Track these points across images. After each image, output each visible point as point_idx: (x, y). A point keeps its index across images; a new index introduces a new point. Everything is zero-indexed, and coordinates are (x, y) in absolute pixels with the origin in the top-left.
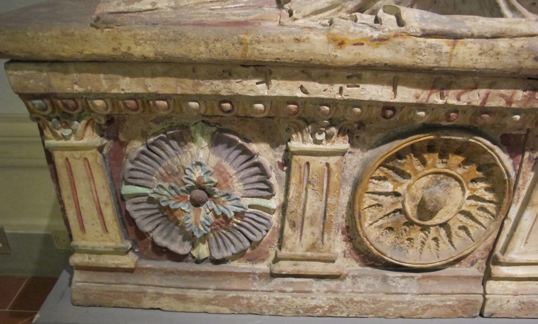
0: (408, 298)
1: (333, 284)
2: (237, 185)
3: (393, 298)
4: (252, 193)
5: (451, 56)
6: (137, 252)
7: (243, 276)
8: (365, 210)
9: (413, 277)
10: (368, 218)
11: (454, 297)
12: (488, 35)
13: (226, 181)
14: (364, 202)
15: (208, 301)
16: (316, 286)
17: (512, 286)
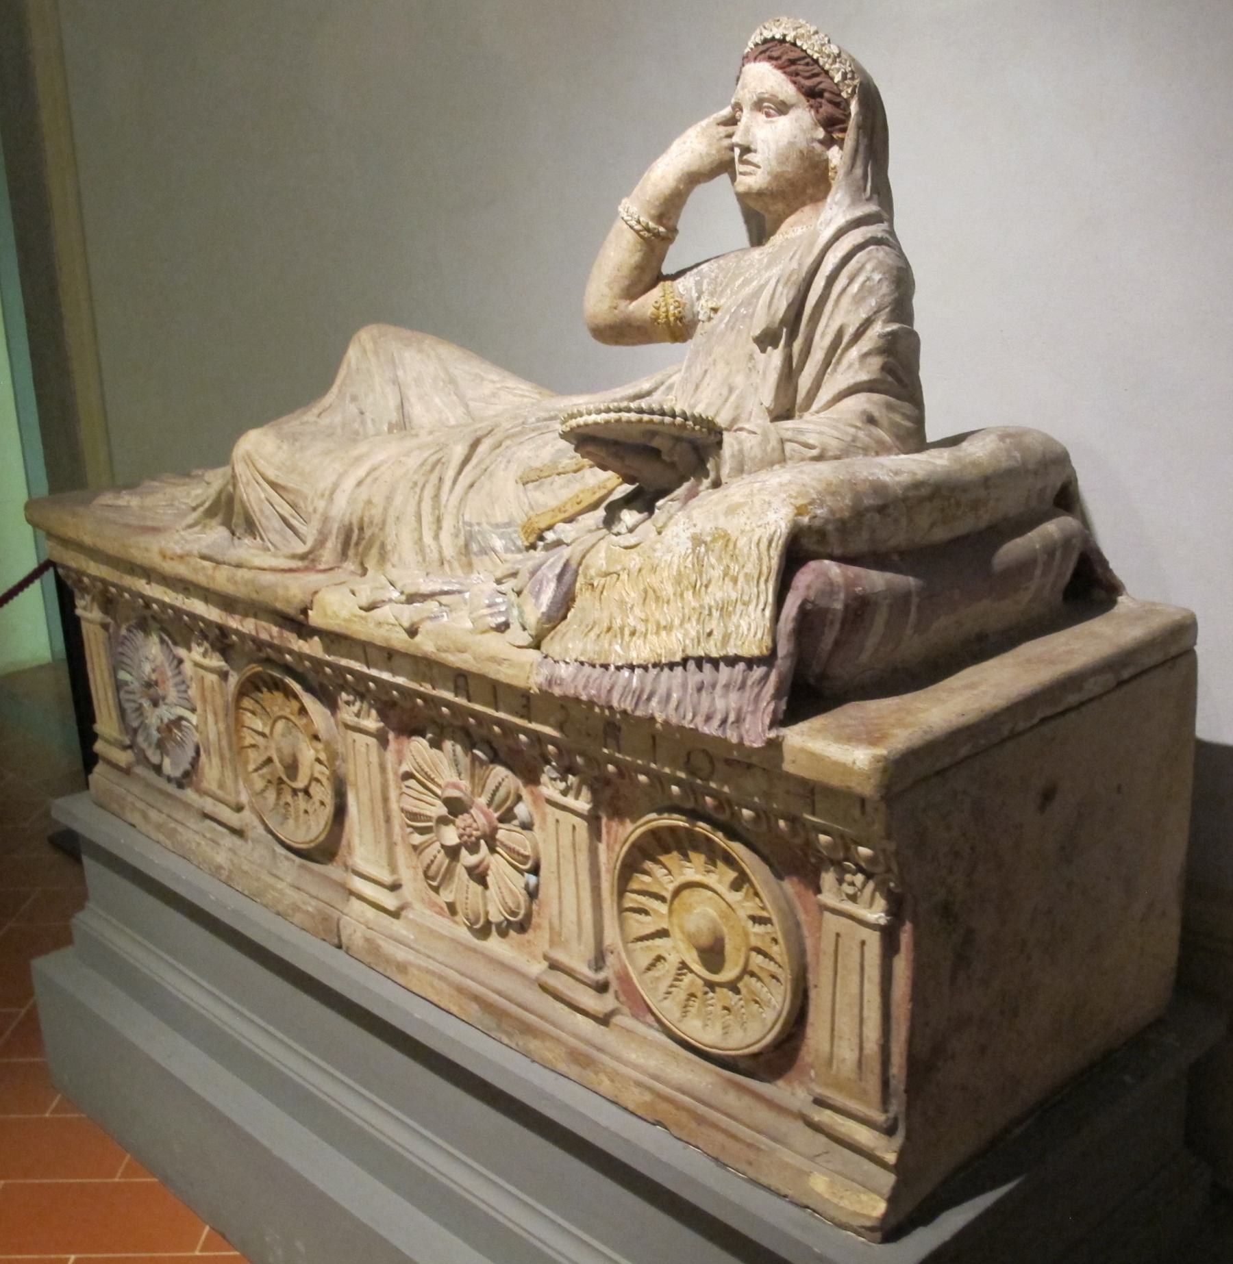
0: (280, 885)
1: (237, 841)
2: (171, 689)
3: (271, 880)
4: (182, 702)
5: (213, 578)
6: (135, 753)
7: (187, 806)
8: (249, 750)
9: (293, 861)
10: (251, 761)
11: (314, 902)
12: (233, 563)
13: (164, 682)
14: (245, 738)
15: (159, 827)
16: (229, 840)
17: (371, 913)
